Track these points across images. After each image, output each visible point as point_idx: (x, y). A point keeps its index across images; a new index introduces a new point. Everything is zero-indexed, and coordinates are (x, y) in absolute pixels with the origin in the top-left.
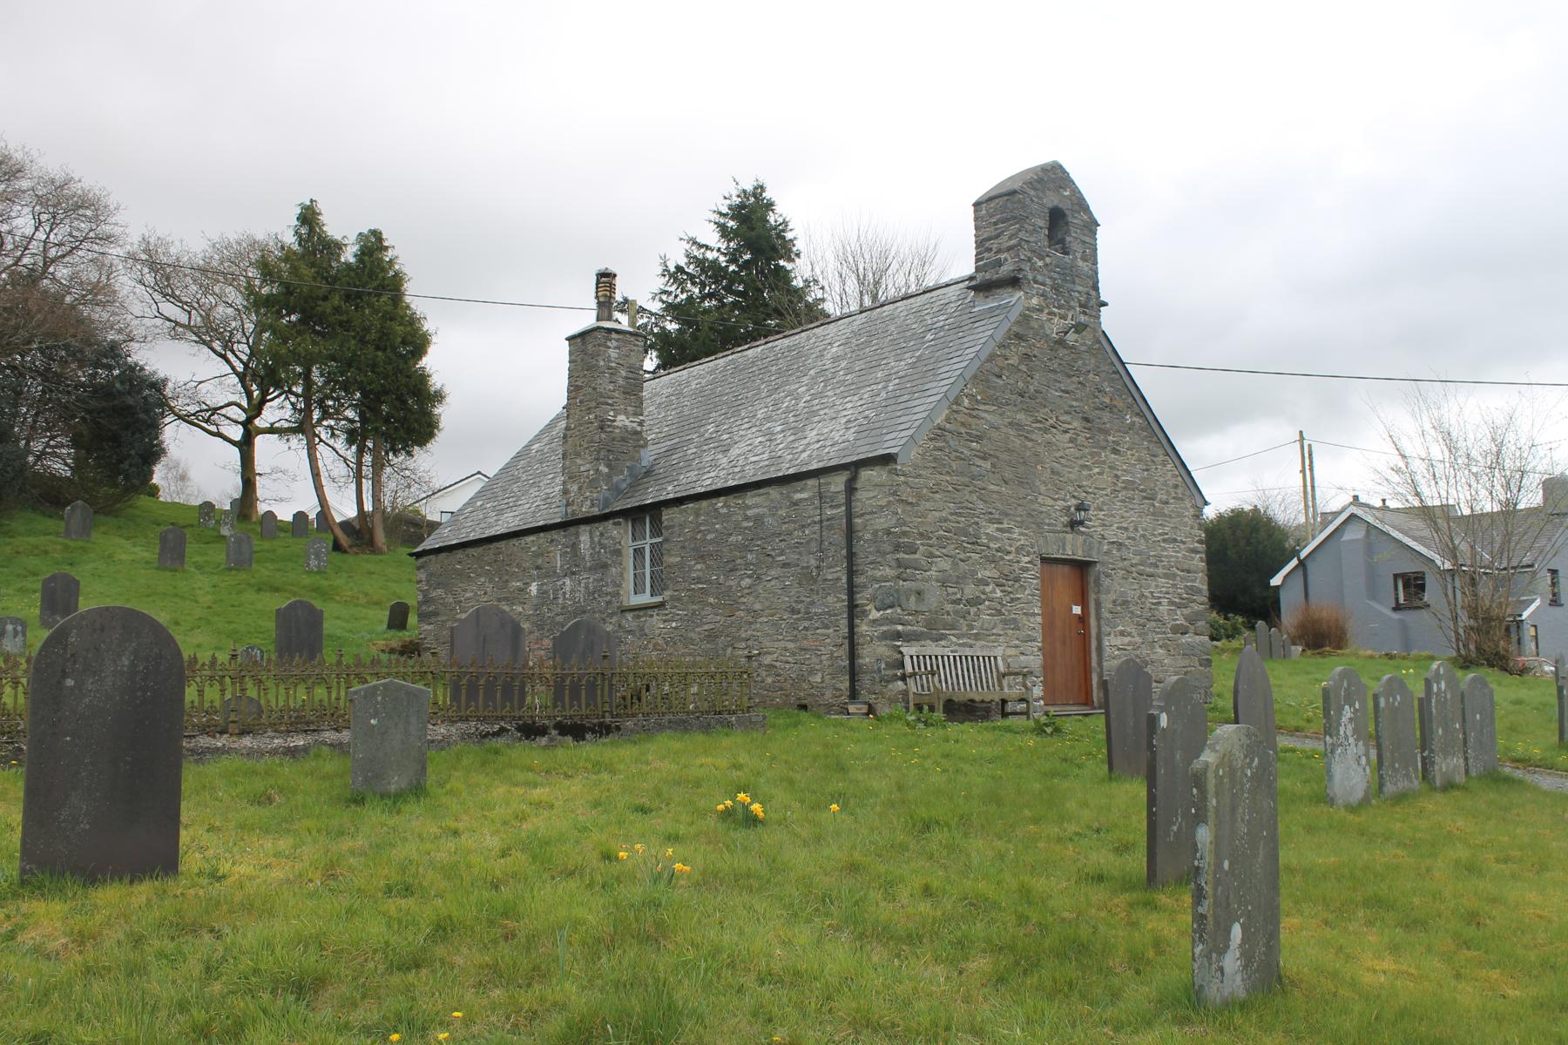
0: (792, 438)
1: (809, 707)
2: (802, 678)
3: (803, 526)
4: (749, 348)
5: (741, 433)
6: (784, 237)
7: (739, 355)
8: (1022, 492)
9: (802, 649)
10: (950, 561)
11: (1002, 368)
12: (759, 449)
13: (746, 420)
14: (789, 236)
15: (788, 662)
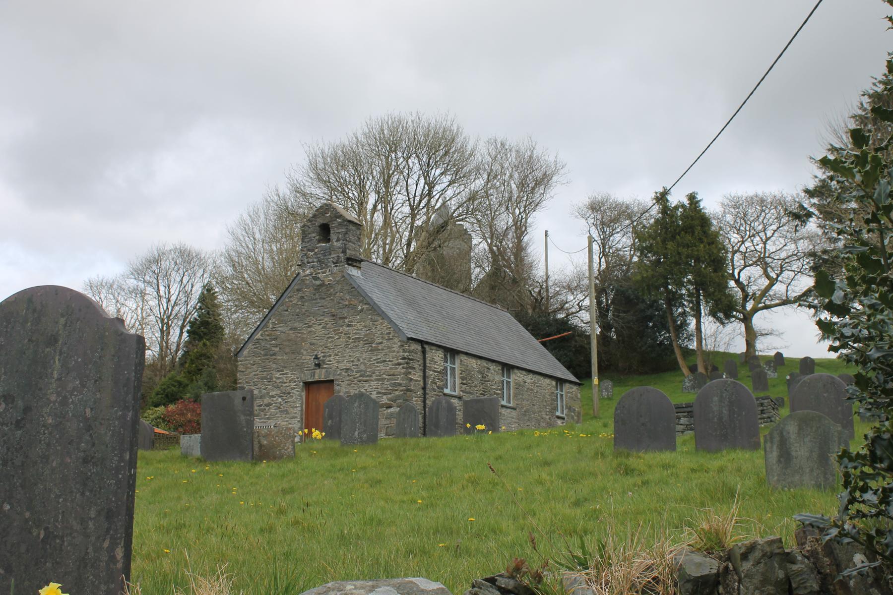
8: (293, 356)
10: (258, 390)
11: (288, 307)
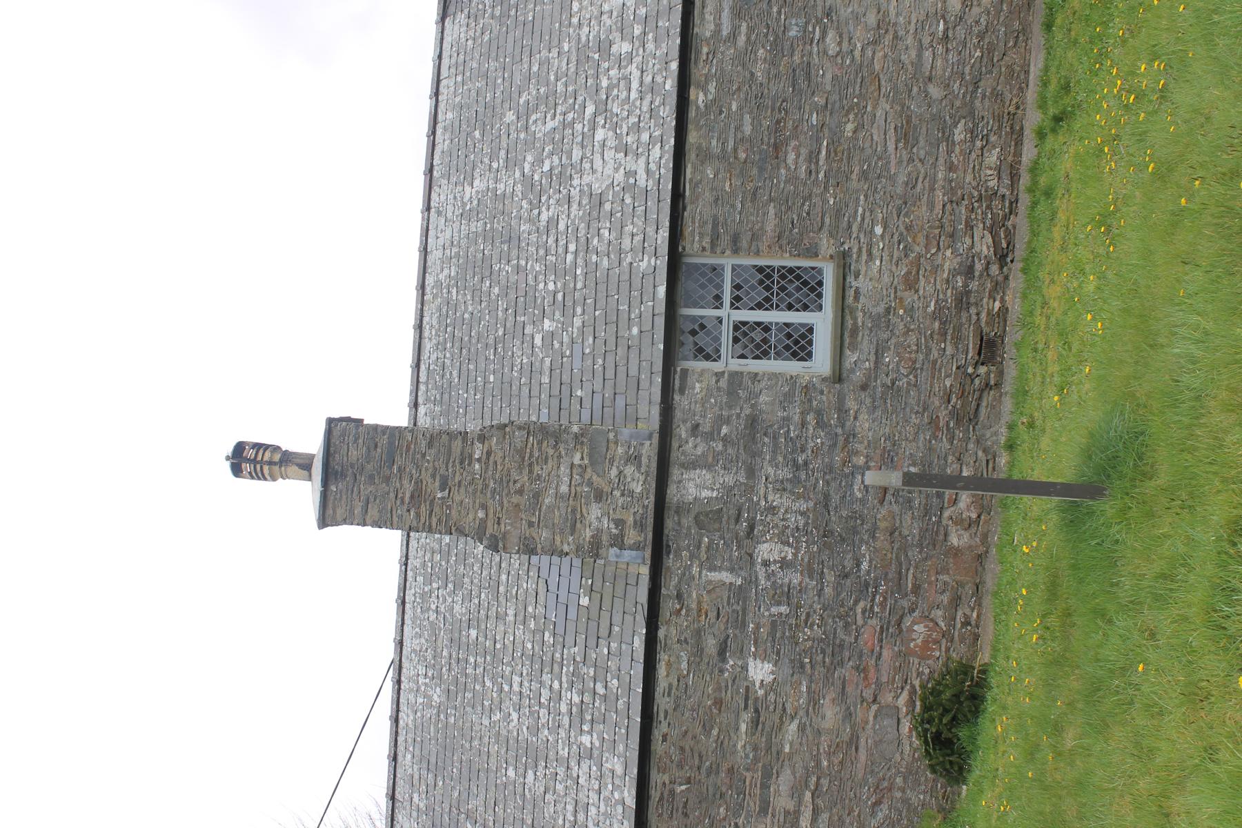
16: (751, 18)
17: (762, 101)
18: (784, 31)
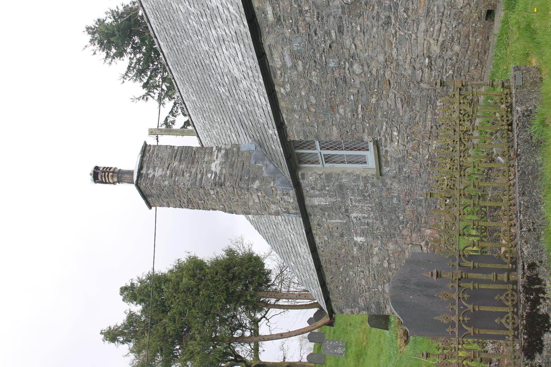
0: (219, 20)
1: (490, 8)
2: (458, 16)
3: (301, 12)
4: (162, 51)
5: (221, 65)
6: (122, 13)
7: (167, 60)
9: (427, 15)
12: (232, 51)
13: (211, 60)
14: (121, 9)
15: (440, 30)
16: (304, 58)
17: (319, 91)
18: (326, 64)
